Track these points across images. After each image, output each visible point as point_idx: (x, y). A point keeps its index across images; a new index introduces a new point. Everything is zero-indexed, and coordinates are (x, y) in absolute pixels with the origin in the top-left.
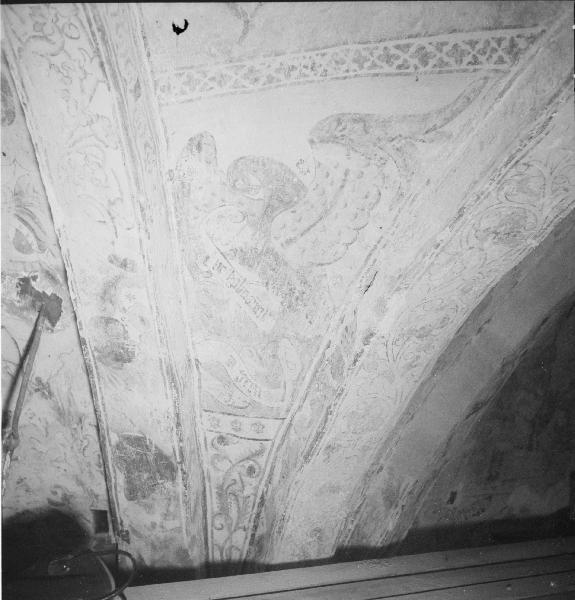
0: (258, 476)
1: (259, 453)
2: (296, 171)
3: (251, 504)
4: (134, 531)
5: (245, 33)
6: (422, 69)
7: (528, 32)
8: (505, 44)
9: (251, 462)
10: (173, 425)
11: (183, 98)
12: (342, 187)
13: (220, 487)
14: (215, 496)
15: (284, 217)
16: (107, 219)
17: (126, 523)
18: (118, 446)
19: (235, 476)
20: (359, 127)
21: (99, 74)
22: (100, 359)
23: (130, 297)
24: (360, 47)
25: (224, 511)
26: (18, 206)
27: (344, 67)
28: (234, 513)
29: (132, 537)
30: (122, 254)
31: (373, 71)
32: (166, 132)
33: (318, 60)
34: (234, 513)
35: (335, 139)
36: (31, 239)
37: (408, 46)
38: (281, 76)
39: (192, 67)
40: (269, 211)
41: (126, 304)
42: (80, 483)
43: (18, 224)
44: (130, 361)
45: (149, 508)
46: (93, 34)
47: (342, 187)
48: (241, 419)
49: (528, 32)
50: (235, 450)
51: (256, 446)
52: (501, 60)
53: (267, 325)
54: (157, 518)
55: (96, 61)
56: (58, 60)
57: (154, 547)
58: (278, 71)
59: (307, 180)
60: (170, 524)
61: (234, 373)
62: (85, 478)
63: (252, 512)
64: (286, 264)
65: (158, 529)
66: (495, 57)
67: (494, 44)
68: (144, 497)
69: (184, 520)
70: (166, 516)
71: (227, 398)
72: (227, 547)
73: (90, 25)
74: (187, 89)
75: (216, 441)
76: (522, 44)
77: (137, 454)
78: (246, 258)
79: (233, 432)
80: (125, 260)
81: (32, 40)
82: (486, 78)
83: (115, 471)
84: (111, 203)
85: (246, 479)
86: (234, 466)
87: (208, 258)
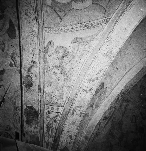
0: (57, 122)
1: (57, 116)
2: (68, 48)
3: (54, 130)
4: (26, 133)
5: (61, 22)
6: (92, 27)
7: (109, 17)
8: (106, 20)
9: (55, 119)
10: (39, 103)
11: (49, 33)
12: (77, 51)
13: (47, 125)
14: (46, 128)
15: (66, 59)
16: (32, 52)
17: (25, 130)
18: (26, 109)
19: (51, 122)
20: (80, 39)
21: (36, 22)
22: (25, 86)
23: (34, 70)
24: (81, 24)
25: (48, 132)
26: (12, 56)
27: (78, 28)
28: (50, 133)
29: (26, 135)
30: (34, 60)
31: (83, 29)
32: (45, 40)
33: (73, 27)
34: (50, 133)
35: (76, 42)
36: (13, 64)
37: (89, 23)
38: (67, 30)
39: (51, 27)
40: (63, 57)
41: (33, 72)
42: (14, 125)
43: (11, 60)
44: (32, 86)
45: (31, 126)
46: (36, 14)
47: (77, 51)
48: (53, 107)
49: (109, 17)
50: (52, 115)
51: (56, 114)
52: (105, 23)
53: (61, 84)
54: (33, 129)
55: (36, 19)
56: (28, 19)
57: (31, 137)
58: (66, 30)
59: (70, 50)
60: (36, 130)
61: (53, 95)
62: (15, 123)
63: (54, 132)
64: (65, 69)
65: (33, 132)
66: (104, 23)
67: (104, 21)
68: (30, 123)
69: (39, 129)
70: (35, 128)
71: (51, 101)
72: (48, 142)
73: (36, 12)
74: (49, 32)
75: (47, 113)
76: (108, 20)
77: (30, 111)
78: (57, 67)
79: (51, 110)
80: (34, 61)
81: (25, 15)
82: (103, 27)
83: (24, 116)
84: (33, 49)
85: (54, 123)
86: (51, 119)
87: (50, 67)
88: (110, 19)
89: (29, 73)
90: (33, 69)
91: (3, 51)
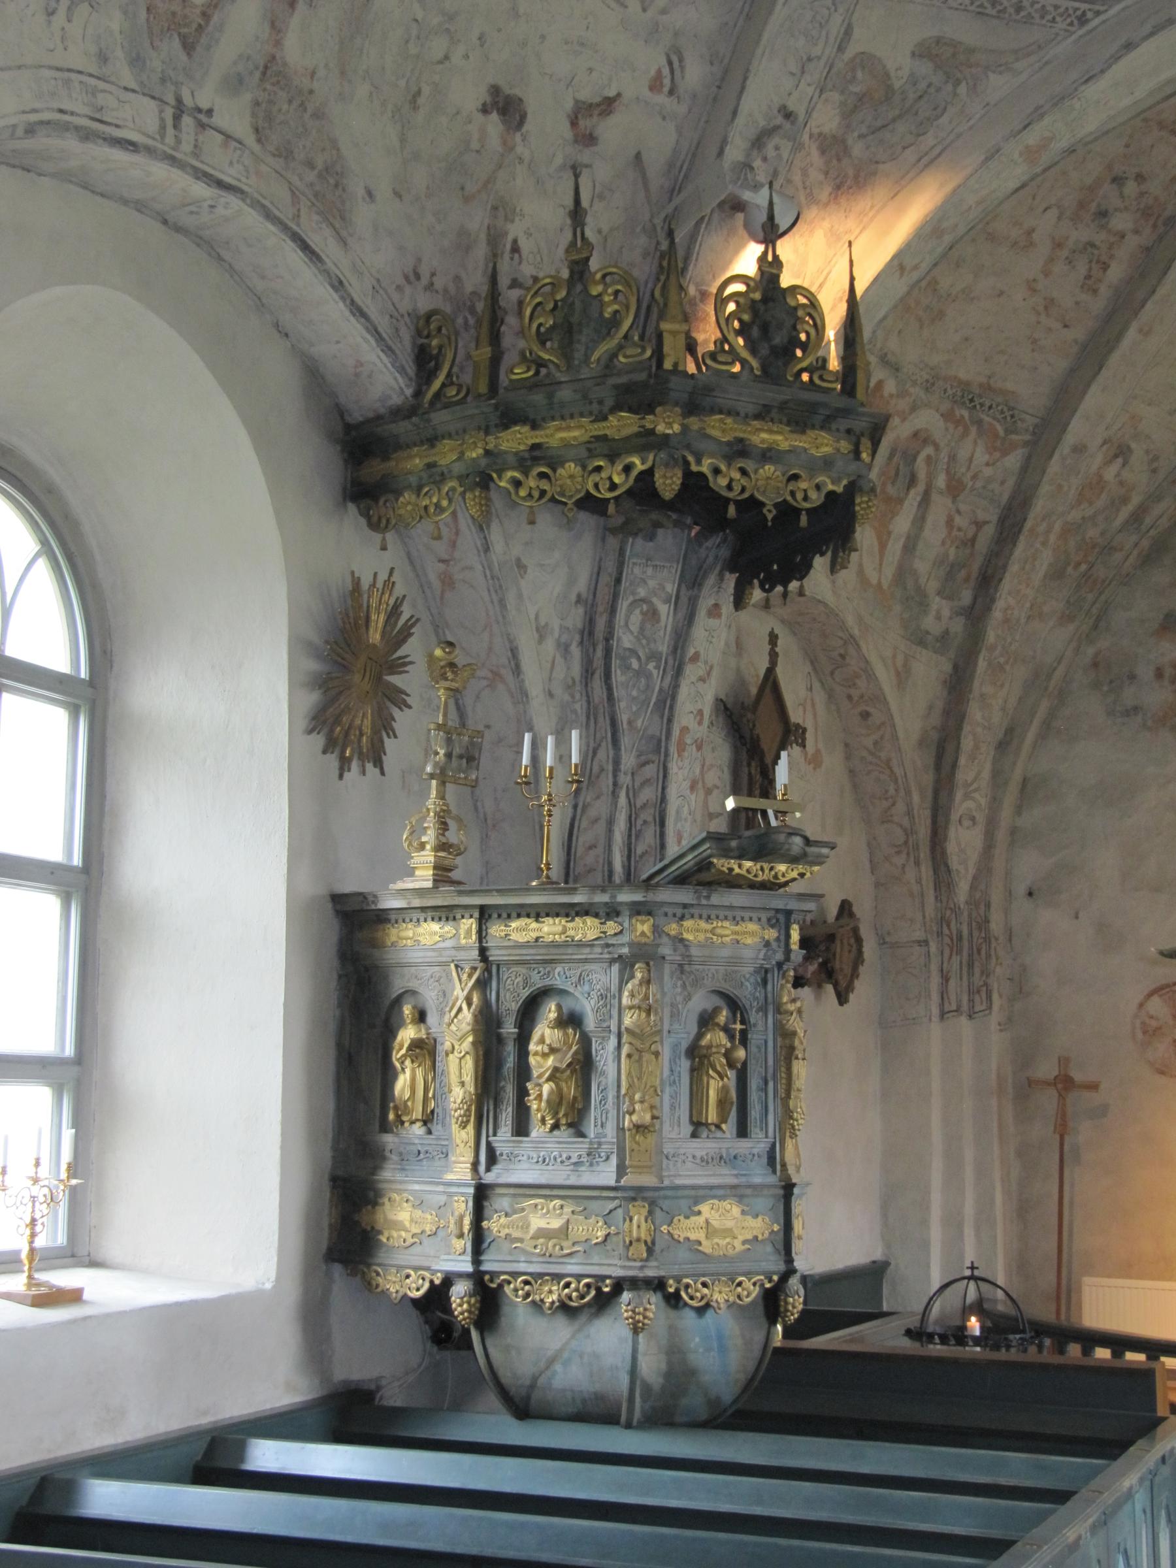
2: (892, 74)
6: (1014, 17)
8: (1079, 13)
23: (777, 148)
30: (791, 107)
31: (979, 10)
36: (667, 82)
49: (1097, 7)
52: (1071, 24)
66: (1069, 20)
67: (1071, 11)
76: (1089, 15)
82: (1057, 34)
88: (1098, 13)
89: (755, 152)
90: (776, 140)
91: (644, 10)
